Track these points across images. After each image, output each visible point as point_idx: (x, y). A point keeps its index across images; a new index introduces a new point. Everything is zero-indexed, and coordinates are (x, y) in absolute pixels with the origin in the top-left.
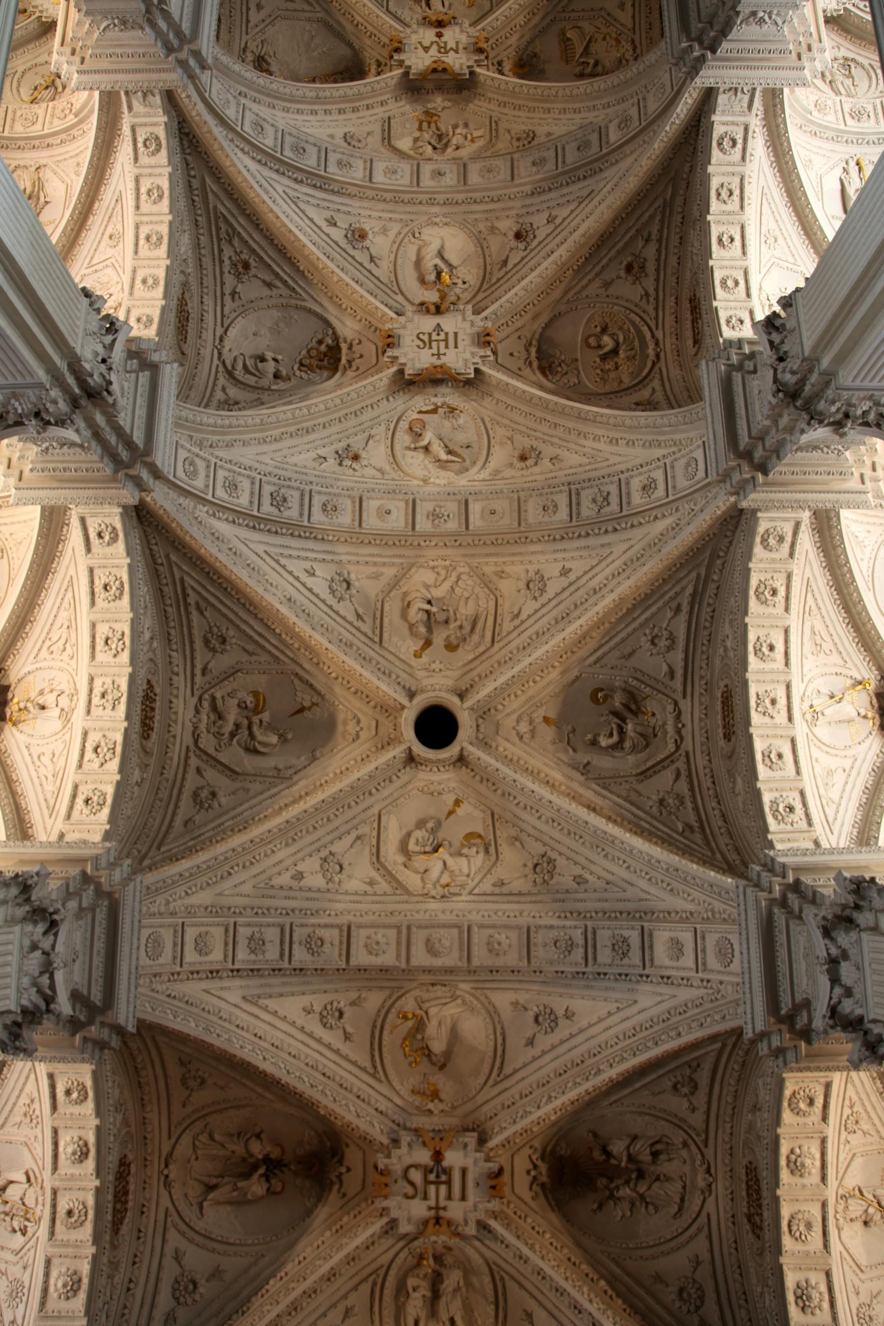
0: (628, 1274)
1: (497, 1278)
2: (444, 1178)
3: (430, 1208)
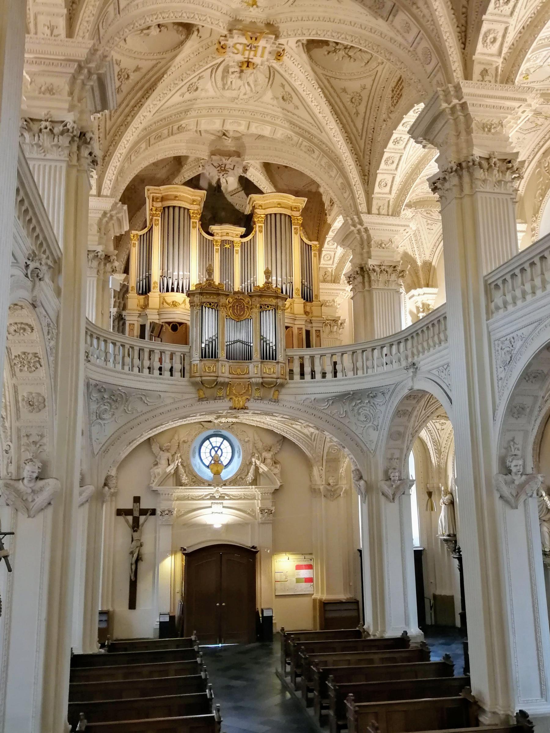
0: (332, 87)
1: (272, 71)
2: (253, 49)
3: (245, 58)
